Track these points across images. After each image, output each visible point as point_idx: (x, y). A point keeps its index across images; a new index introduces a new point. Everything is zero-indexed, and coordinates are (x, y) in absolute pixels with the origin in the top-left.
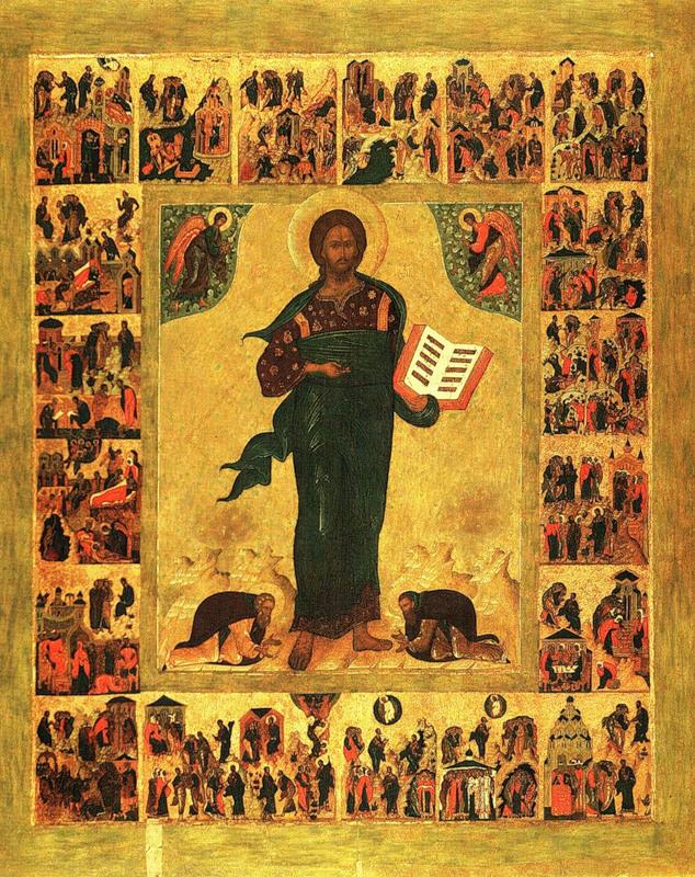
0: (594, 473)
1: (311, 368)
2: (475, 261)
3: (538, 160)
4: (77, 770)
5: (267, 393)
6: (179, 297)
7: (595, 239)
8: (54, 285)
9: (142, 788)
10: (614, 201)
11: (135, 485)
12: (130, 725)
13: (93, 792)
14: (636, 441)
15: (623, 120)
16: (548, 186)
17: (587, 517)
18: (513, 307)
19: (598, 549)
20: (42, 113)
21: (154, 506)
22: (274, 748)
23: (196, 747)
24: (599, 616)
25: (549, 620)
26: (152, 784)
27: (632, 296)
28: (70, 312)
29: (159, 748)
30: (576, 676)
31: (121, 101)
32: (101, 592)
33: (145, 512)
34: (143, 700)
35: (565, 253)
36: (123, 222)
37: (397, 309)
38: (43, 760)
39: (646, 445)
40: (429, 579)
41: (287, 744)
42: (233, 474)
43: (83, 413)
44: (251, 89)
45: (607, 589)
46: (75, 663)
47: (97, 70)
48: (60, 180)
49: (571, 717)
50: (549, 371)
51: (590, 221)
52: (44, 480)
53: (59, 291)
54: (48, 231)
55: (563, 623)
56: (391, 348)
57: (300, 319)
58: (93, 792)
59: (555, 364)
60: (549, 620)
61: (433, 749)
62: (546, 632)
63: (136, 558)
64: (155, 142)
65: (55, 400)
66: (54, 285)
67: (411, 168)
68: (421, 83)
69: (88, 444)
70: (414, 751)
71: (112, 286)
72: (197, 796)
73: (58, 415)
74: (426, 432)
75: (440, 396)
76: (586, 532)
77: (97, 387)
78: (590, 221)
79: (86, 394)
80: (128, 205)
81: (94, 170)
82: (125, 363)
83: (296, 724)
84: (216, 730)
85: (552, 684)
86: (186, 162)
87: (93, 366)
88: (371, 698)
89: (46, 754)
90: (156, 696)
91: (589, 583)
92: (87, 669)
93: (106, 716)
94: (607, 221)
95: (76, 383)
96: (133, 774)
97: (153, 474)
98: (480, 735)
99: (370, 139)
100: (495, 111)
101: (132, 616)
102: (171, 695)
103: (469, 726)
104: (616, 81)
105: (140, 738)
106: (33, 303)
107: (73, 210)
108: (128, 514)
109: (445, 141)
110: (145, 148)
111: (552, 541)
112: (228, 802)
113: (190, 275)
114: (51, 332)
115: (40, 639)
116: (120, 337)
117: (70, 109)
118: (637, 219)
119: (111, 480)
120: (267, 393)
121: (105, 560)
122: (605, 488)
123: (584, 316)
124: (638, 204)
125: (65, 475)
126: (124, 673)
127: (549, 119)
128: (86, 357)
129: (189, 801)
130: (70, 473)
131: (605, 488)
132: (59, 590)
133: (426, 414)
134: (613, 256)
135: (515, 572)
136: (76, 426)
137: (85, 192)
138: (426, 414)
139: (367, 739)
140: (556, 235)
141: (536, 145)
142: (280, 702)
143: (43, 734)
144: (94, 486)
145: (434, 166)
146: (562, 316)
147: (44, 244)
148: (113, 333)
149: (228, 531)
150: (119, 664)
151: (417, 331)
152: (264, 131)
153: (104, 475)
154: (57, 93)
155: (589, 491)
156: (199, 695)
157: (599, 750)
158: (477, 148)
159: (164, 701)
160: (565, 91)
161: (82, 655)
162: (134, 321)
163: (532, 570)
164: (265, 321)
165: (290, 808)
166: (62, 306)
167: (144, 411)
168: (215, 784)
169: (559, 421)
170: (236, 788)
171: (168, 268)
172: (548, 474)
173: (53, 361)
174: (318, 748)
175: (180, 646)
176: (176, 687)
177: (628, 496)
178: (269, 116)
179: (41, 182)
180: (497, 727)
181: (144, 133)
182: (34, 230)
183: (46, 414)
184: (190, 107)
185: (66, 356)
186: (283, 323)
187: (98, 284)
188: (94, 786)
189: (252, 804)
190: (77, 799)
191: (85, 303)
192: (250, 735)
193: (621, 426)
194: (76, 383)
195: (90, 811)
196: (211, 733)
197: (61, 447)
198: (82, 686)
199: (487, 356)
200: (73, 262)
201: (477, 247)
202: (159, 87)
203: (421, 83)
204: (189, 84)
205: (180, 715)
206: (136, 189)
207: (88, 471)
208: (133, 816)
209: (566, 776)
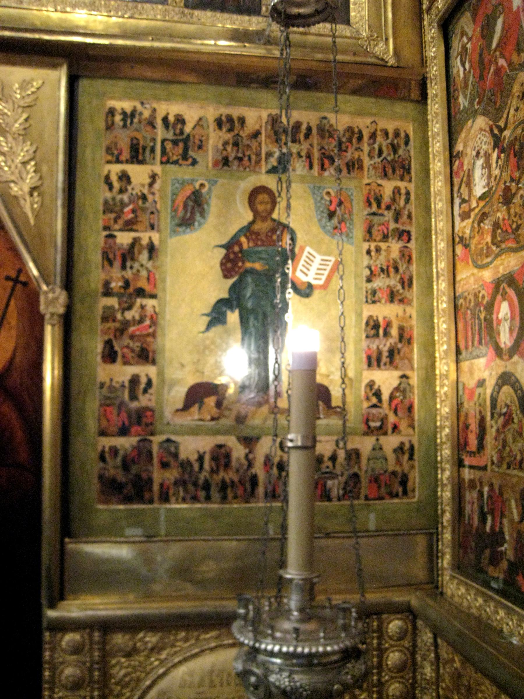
0: (388, 324)
1: (248, 265)
2: (331, 215)
3: (361, 168)
4: (121, 477)
5: (226, 277)
6: (180, 225)
7: (388, 208)
8: (113, 216)
9: (156, 488)
10: (397, 191)
11: (154, 322)
12: (150, 454)
13: (129, 490)
14: (408, 309)
15: (401, 152)
16: (366, 181)
19: (391, 362)
20: (110, 127)
21: (164, 335)
22: (227, 465)
23: (186, 465)
24: (392, 398)
25: (368, 399)
26: (162, 485)
27: (405, 237)
28: (121, 230)
29: (165, 465)
30: (380, 428)
31: (151, 124)
32: (135, 381)
33: (159, 339)
34: (157, 439)
35: (374, 214)
36: (151, 185)
38: (102, 472)
39: (413, 311)
42: (207, 319)
43: (127, 284)
45: (395, 383)
46: (120, 419)
48: (118, 161)
49: (378, 448)
50: (367, 272)
51: (386, 199)
52: (105, 319)
55: (374, 400)
57: (243, 239)
59: (369, 267)
60: (368, 399)
62: (366, 405)
63: (154, 362)
64: (169, 146)
65: (111, 277)
66: (113, 216)
68: (304, 127)
69: (129, 301)
71: (144, 218)
72: (186, 491)
73: (113, 285)
74: (306, 300)
75: (314, 282)
76: (385, 354)
77: (134, 271)
78: (386, 199)
79: (129, 274)
80: (153, 177)
82: (150, 258)
84: (196, 456)
85: (369, 431)
86: (185, 157)
87: (133, 259)
89: (105, 469)
90: (164, 437)
92: (127, 422)
93: (137, 448)
94: (394, 200)
95: (123, 267)
96: (150, 480)
97: (164, 318)
98: (333, 458)
100: (340, 143)
101: (151, 394)
102: (173, 438)
104: (397, 134)
105: (156, 461)
106: (101, 224)
107: (125, 177)
108: (150, 339)
109: (316, 155)
111: (369, 358)
112: (202, 494)
113: (186, 212)
114: (110, 241)
115: (101, 405)
116: (148, 245)
117: (125, 126)
118: (407, 200)
119: (141, 321)
120: (226, 277)
121: (138, 363)
122: (394, 332)
123: (383, 246)
124: (408, 193)
125: (115, 317)
126: (147, 425)
127: (366, 148)
129: (182, 494)
130: (119, 316)
131: (394, 332)
132: (111, 380)
134: (397, 217)
136: (122, 291)
137: (132, 169)
139: (276, 460)
140: (370, 205)
141: (360, 161)
142: (231, 441)
143: (102, 458)
144: (132, 323)
145: (311, 167)
146: (373, 245)
147: (108, 195)
148: (145, 242)
150: (144, 420)
151: (302, 249)
152: (226, 144)
153: (137, 317)
154: (118, 118)
155: (386, 334)
156: (187, 437)
157: (392, 466)
158: (332, 160)
159: (168, 441)
160: (373, 136)
161: (124, 415)
162: (156, 237)
163: (359, 374)
164: (225, 240)
165: (235, 497)
166: (117, 227)
167: (159, 285)
168: (195, 484)
170: (207, 487)
171: (174, 210)
172: (367, 324)
173: (111, 256)
174: (250, 465)
175: (178, 411)
178: (228, 136)
180: (341, 455)
181: (163, 141)
183: (107, 284)
184: (188, 129)
185: (118, 253)
187: (136, 217)
188: (130, 486)
190: (120, 493)
191: (129, 226)
192: (215, 458)
193: (401, 301)
194: (123, 267)
195: (128, 500)
196: (194, 457)
197: (113, 302)
198: (124, 432)
200: (123, 204)
201: (332, 208)
202: (171, 119)
203: (304, 127)
204: (187, 117)
205: (177, 448)
206: (158, 169)
207: (129, 315)
208: (151, 502)
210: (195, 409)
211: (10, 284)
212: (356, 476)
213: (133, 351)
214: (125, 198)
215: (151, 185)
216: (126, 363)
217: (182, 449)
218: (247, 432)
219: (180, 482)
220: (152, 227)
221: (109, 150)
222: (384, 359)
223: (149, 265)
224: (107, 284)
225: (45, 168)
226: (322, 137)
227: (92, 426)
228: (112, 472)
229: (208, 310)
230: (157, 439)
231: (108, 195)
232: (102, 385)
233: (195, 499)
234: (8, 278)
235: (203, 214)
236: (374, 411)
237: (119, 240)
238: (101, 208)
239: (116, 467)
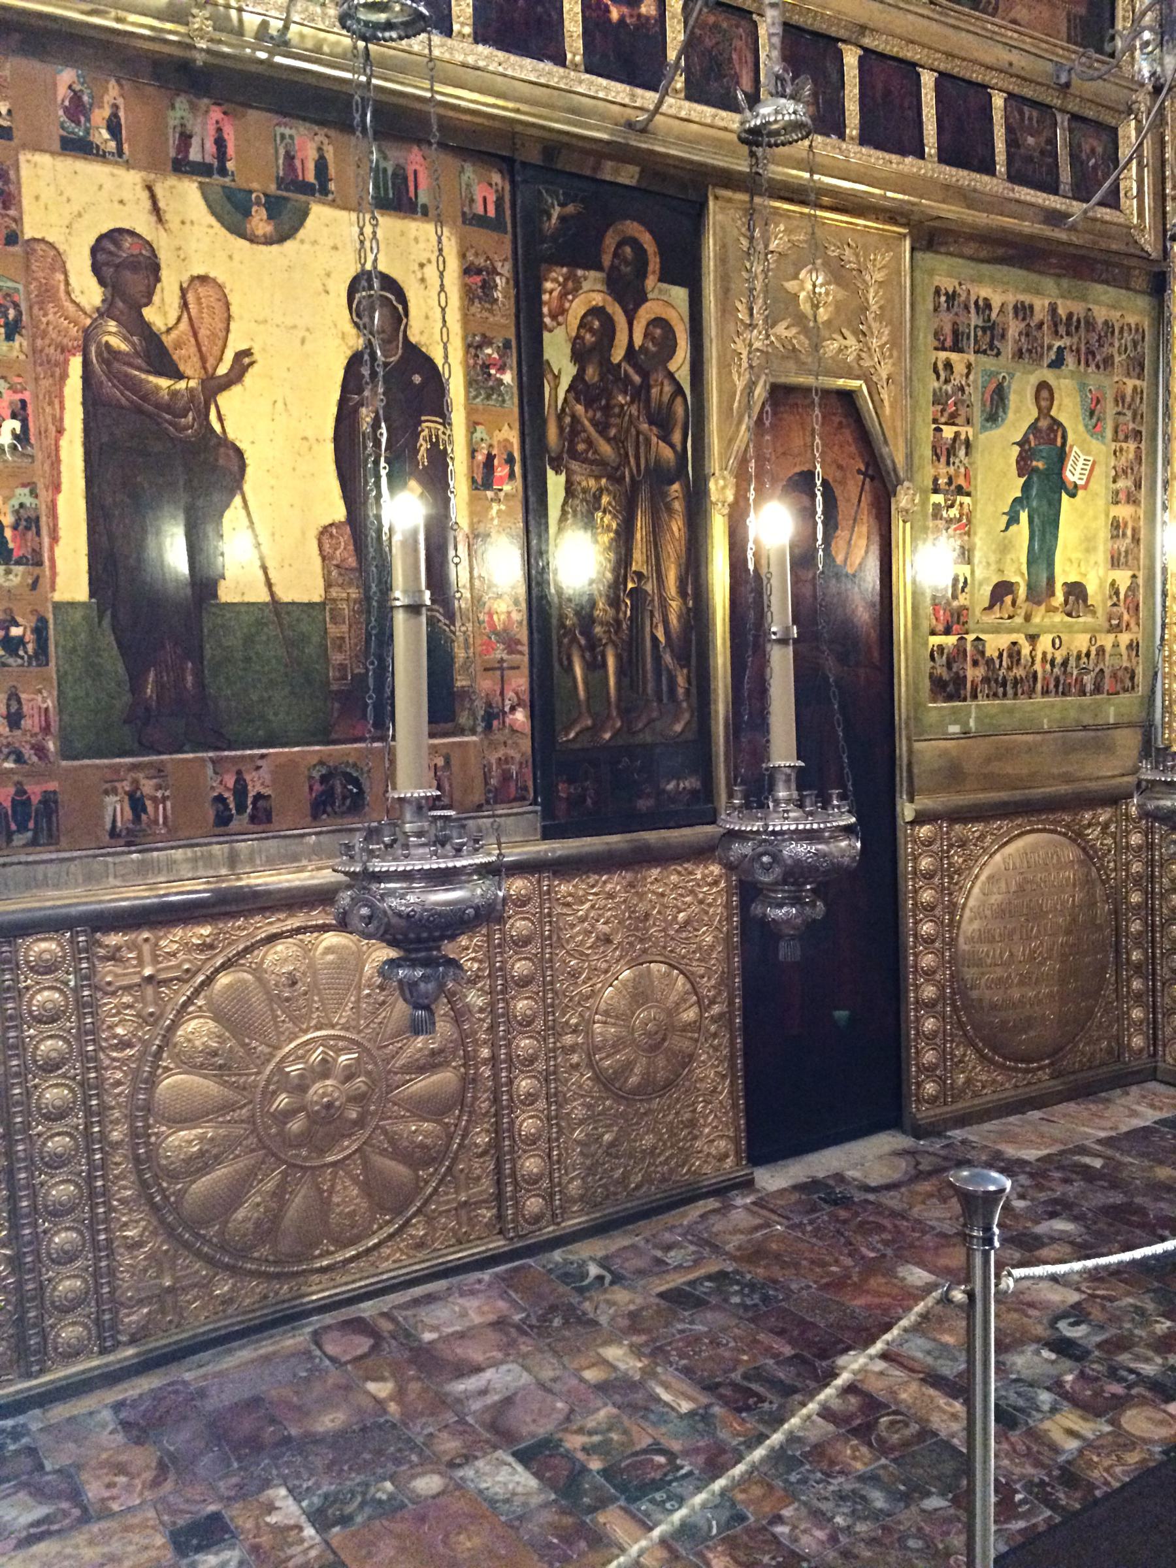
2: (1092, 414)
4: (946, 676)
5: (1020, 475)
6: (987, 420)
8: (940, 407)
23: (990, 662)
29: (975, 663)
40: (1072, 579)
41: (1023, 661)
48: (944, 349)
49: (1116, 645)
50: (1113, 473)
53: (943, 411)
56: (1061, 456)
58: (950, 688)
61: (1072, 662)
62: (1110, 603)
66: (940, 407)
67: (1070, 359)
70: (1065, 663)
75: (1079, 483)
79: (952, 470)
86: (991, 346)
88: (1050, 637)
91: (1123, 578)
98: (1088, 655)
99: (1057, 344)
102: (982, 636)
103: (1084, 651)
106: (931, 417)
107: (948, 365)
117: (948, 309)
119: (960, 520)
120: (1020, 475)
137: (954, 357)
139: (1049, 657)
143: (932, 658)
147: (936, 385)
148: (963, 437)
149: (1004, 549)
152: (1020, 334)
159: (978, 639)
168: (996, 681)
171: (984, 405)
174: (1033, 663)
176: (984, 632)
179: (936, 349)
181: (976, 327)
183: (936, 480)
184: (994, 315)
189: (1010, 691)
192: (1010, 656)
194: (948, 463)
195: (950, 698)
196: (996, 654)
197: (938, 498)
198: (947, 631)
199: (1094, 463)
202: (981, 303)
206: (972, 357)
208: (965, 700)
210: (997, 608)
212: (1102, 671)
214: (949, 388)
215: (967, 375)
218: (1032, 631)
219: (986, 680)
221: (936, 335)
222: (1122, 560)
223: (966, 461)
226: (1088, 331)
229: (1006, 510)
230: (971, 637)
231: (936, 385)
233: (995, 695)
236: (1115, 609)
237: (945, 435)
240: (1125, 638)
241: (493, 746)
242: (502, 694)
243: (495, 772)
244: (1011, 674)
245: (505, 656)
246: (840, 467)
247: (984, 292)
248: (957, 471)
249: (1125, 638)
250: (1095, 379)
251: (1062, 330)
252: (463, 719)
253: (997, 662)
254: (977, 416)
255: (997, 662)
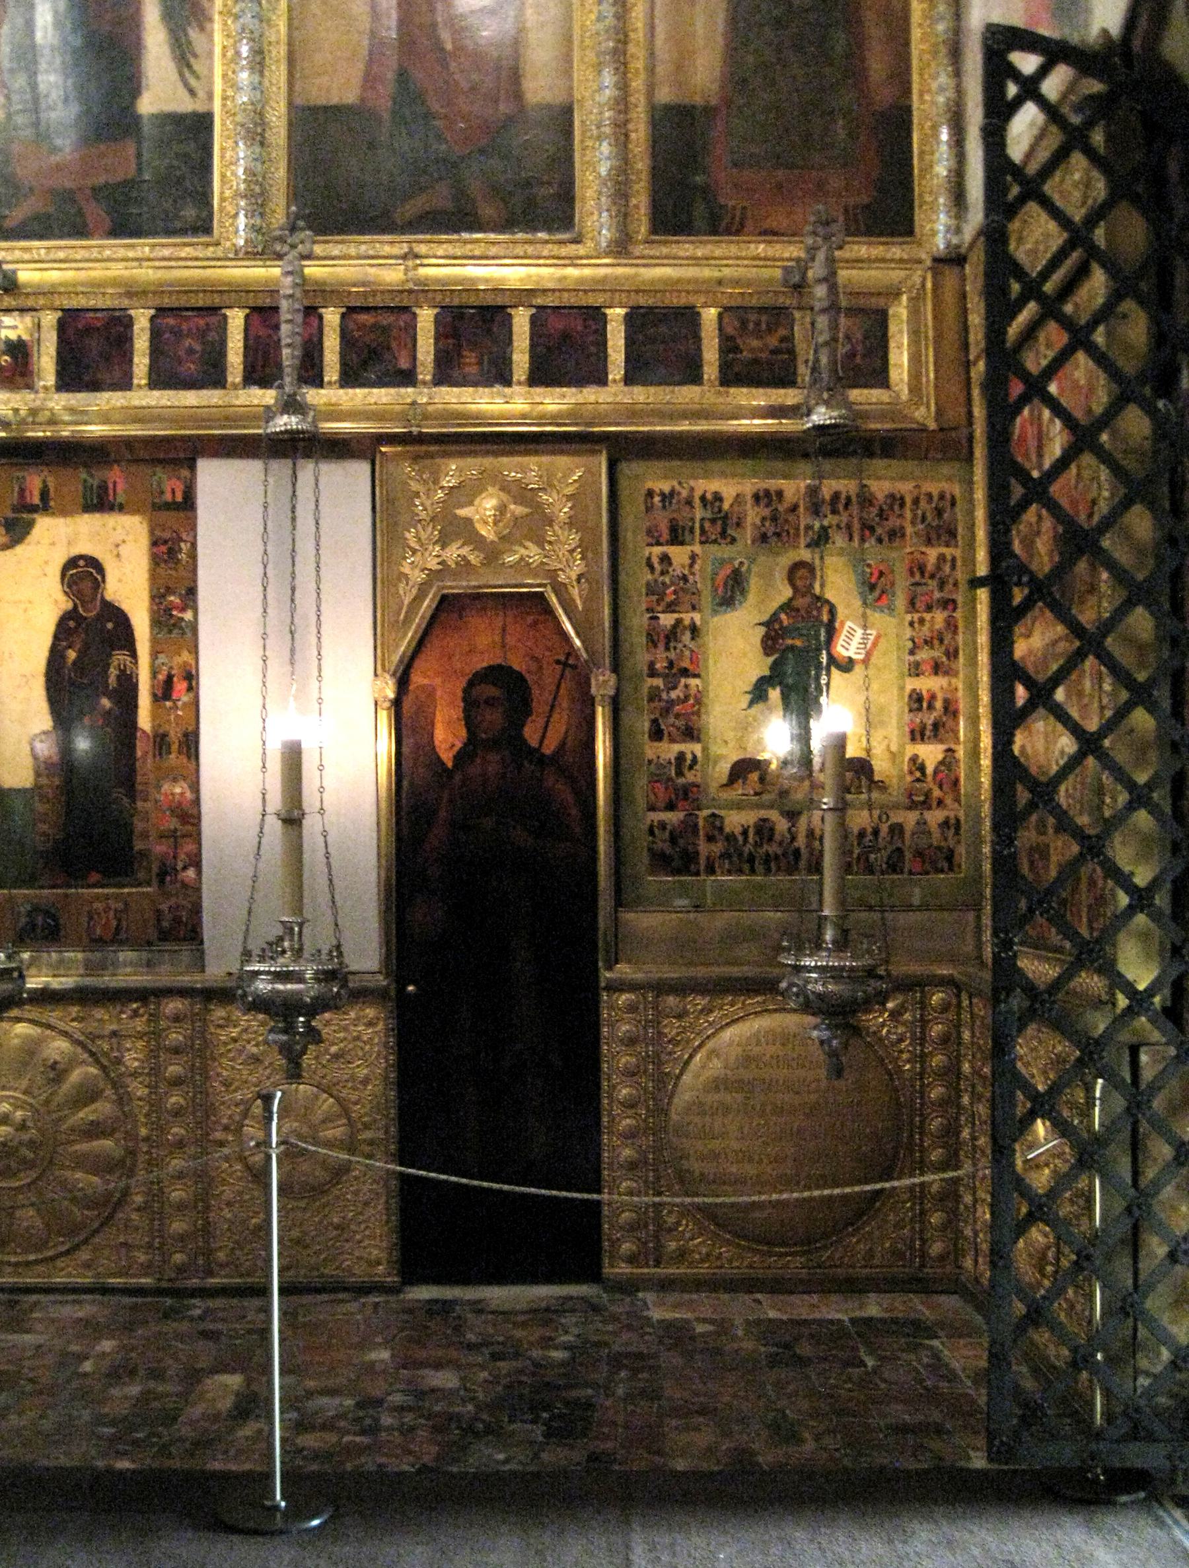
0: (933, 697)
1: (789, 642)
2: (872, 587)
3: (903, 535)
4: (667, 848)
5: (767, 655)
6: (721, 605)
7: (932, 576)
9: (703, 862)
10: (942, 558)
11: (698, 702)
12: (696, 825)
13: (676, 863)
14: (954, 681)
15: (946, 515)
16: (908, 550)
17: (930, 719)
18: (891, 609)
19: (936, 736)
20: (649, 509)
21: (707, 713)
22: (770, 839)
23: (731, 838)
24: (936, 772)
25: (911, 773)
26: (708, 858)
27: (950, 607)
29: (710, 839)
30: (924, 802)
31: (689, 502)
32: (681, 757)
33: (704, 717)
35: (917, 584)
36: (691, 566)
37: (832, 612)
39: (959, 682)
41: (777, 837)
42: (749, 697)
43: (671, 664)
44: (757, 498)
45: (940, 757)
47: (678, 487)
48: (658, 544)
49: (922, 823)
50: (910, 644)
51: (930, 567)
52: (651, 700)
54: (651, 568)
55: (918, 774)
57: (783, 616)
58: (676, 863)
60: (911, 773)
62: (909, 779)
63: (699, 740)
64: (707, 525)
66: (655, 598)
68: (843, 496)
72: (731, 863)
73: (658, 666)
74: (846, 675)
75: (854, 657)
76: (929, 727)
78: (930, 567)
79: (672, 655)
80: (693, 557)
81: (677, 536)
83: (782, 825)
84: (740, 829)
85: (913, 806)
86: (723, 534)
91: (931, 753)
94: (939, 568)
96: (697, 853)
98: (876, 832)
100: (881, 510)
104: (942, 497)
106: (644, 607)
107: (665, 559)
109: (856, 526)
110: (702, 528)
111: (912, 732)
112: (746, 867)
117: (664, 507)
118: (953, 567)
119: (687, 698)
121: (684, 741)
122: (939, 704)
123: (927, 616)
124: (954, 559)
127: (908, 514)
128: (672, 635)
130: (664, 696)
131: (939, 704)
133: (847, 666)
134: (942, 585)
135: (894, 748)
137: (673, 551)
138: (847, 666)
140: (912, 574)
141: (902, 528)
142: (774, 815)
143: (651, 832)
145: (851, 539)
146: (916, 616)
147: (649, 577)
148: (687, 622)
151: (842, 624)
152: (764, 519)
154: (657, 499)
155: (931, 707)
158: (872, 529)
159: (714, 815)
160: (916, 501)
162: (697, 617)
163: (902, 746)
164: (765, 617)
165: (779, 869)
168: (740, 855)
169: (916, 670)
170: (751, 859)
172: (910, 696)
174: (793, 839)
177: (950, 709)
178: (766, 512)
180: (884, 829)
181: (702, 519)
182: (646, 569)
183: (651, 665)
186: (774, 618)
189: (759, 868)
191: (671, 608)
193: (946, 673)
194: (667, 649)
196: (738, 831)
197: (658, 682)
198: (671, 807)
201: (873, 580)
202: (709, 496)
203: (843, 496)
204: (725, 495)
206: (697, 549)
207: (673, 695)
208: (697, 874)
209: (919, 854)
211: (559, 668)
212: (899, 850)
213: (678, 729)
215: (691, 566)
216: (672, 740)
217: (727, 822)
219: (725, 855)
220: (694, 608)
221: (649, 532)
222: (928, 733)
223: (692, 645)
224: (651, 665)
225: (590, 555)
227: (641, 803)
228: (660, 844)
229: (749, 688)
232: (650, 762)
233: (740, 871)
234: (558, 662)
235: (743, 592)
236: (918, 785)
237: (662, 622)
238: (644, 591)
239: (664, 841)
240: (934, 817)
241: (167, 895)
242: (175, 857)
243: (168, 916)
244: (762, 851)
245: (179, 826)
246: (534, 658)
247: (711, 486)
248: (681, 656)
249: (934, 817)
250: (874, 553)
251: (826, 509)
252: (141, 875)
253: (740, 838)
254: (706, 600)
255: (740, 838)
